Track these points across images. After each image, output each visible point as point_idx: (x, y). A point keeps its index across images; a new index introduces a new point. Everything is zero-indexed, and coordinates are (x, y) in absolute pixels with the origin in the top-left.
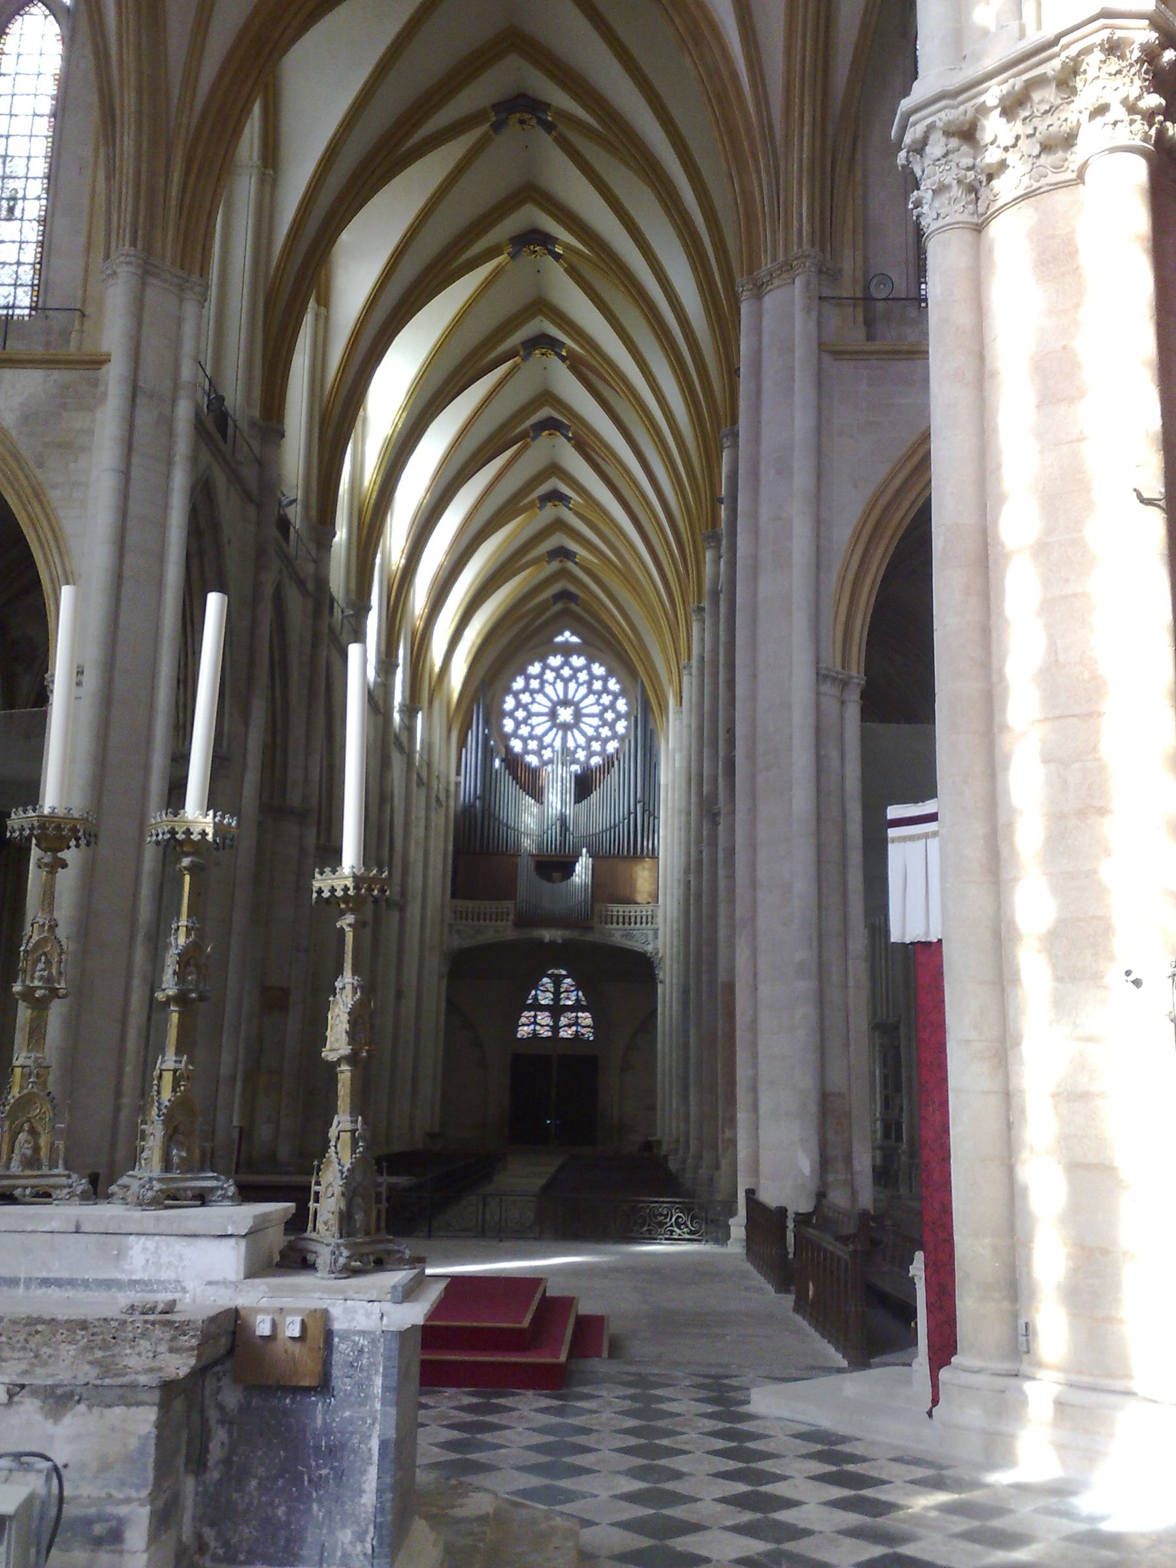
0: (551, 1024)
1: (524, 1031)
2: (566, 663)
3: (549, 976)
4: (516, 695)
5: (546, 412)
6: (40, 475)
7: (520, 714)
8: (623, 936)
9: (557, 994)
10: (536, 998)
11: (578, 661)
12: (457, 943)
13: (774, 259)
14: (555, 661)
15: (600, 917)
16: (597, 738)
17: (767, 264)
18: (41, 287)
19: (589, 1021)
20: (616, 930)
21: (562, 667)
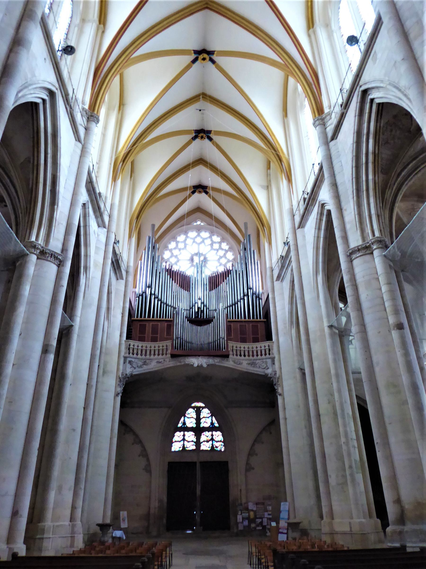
0: (195, 440)
1: (176, 447)
3: (193, 408)
4: (171, 250)
8: (249, 364)
9: (198, 420)
10: (184, 423)
12: (129, 370)
19: (221, 438)
20: (243, 360)
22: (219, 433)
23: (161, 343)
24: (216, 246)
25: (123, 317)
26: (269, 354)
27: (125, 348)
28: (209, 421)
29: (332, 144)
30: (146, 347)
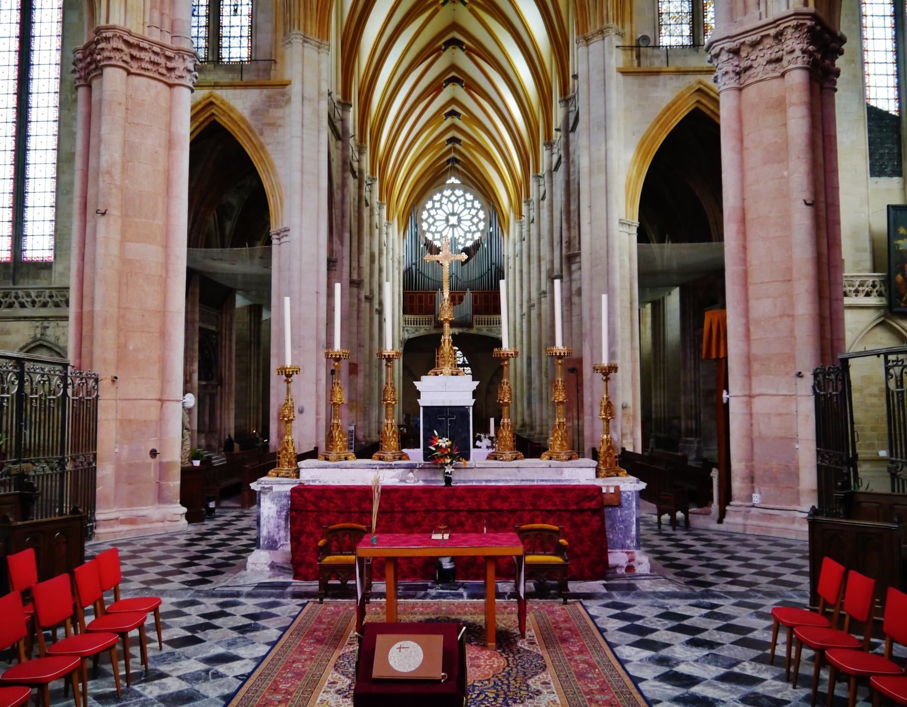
2: (453, 194)
5: (453, 74)
6: (262, 139)
7: (431, 220)
11: (459, 192)
12: (407, 336)
13: (595, 27)
14: (447, 193)
16: (470, 232)
17: (591, 30)
18: (253, 48)
21: (450, 196)
22: (469, 368)
24: (469, 205)
25: (399, 298)
28: (461, 360)
29: (554, 173)
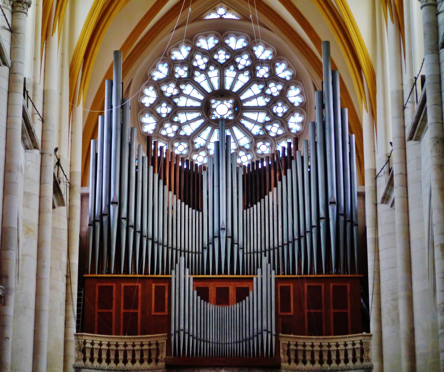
7: (164, 110)
15: (288, 354)
23: (147, 338)
25: (68, 285)
26: (362, 360)
27: (76, 349)
30: (117, 345)
